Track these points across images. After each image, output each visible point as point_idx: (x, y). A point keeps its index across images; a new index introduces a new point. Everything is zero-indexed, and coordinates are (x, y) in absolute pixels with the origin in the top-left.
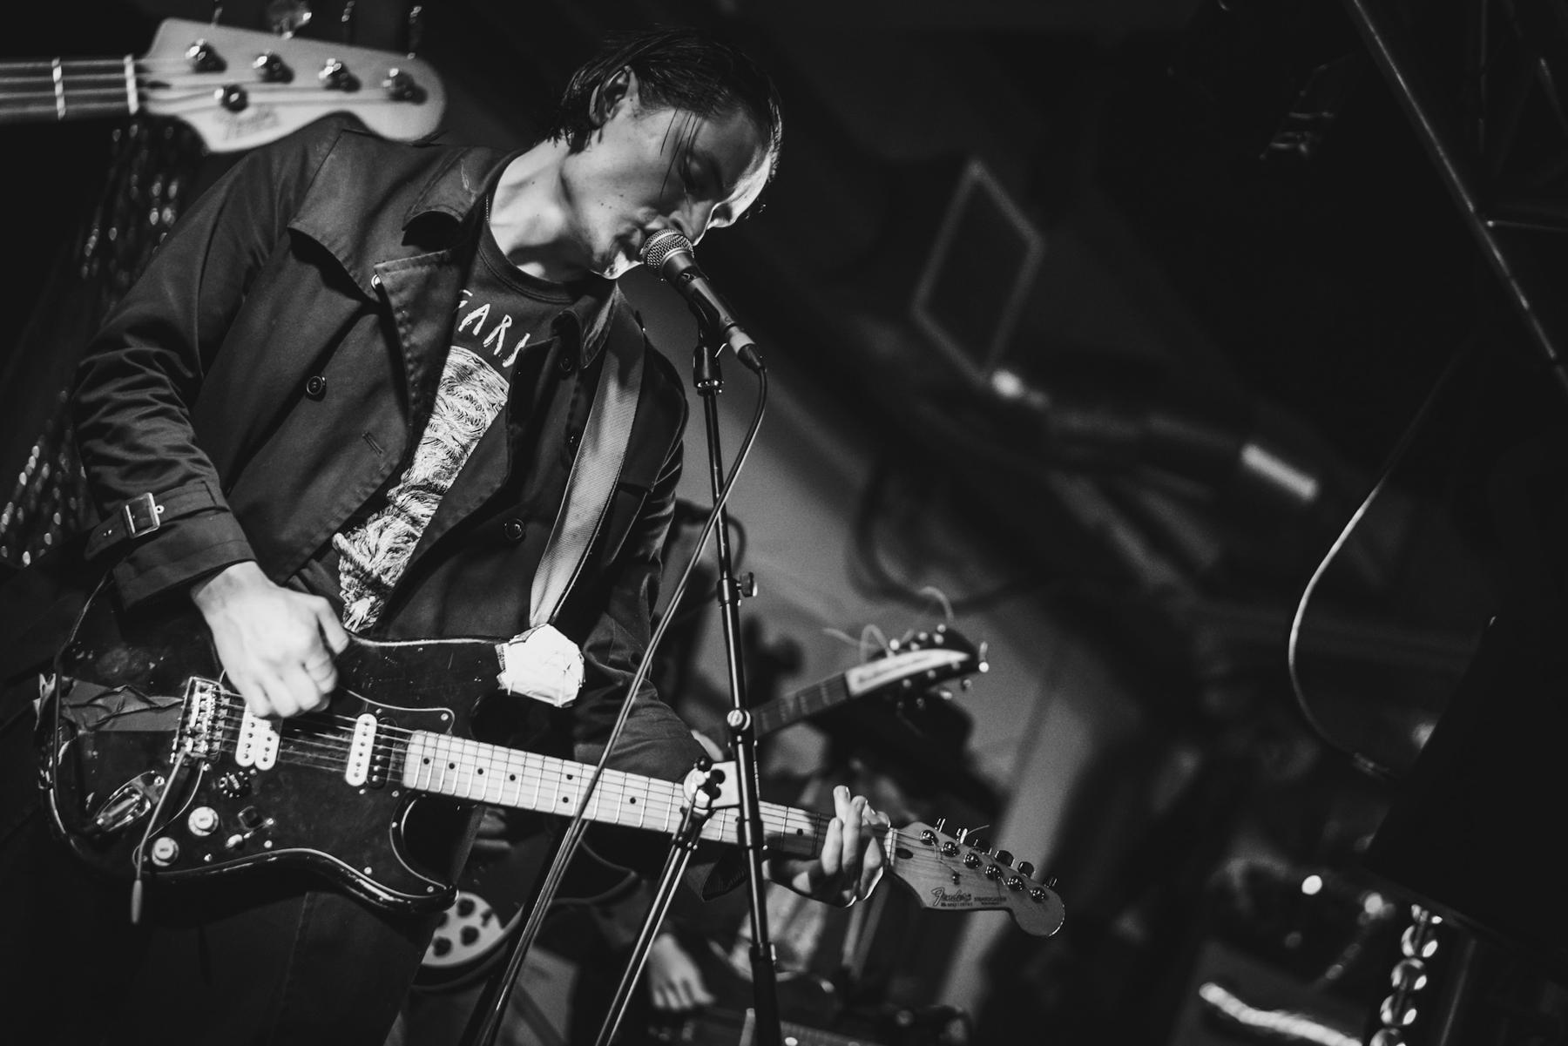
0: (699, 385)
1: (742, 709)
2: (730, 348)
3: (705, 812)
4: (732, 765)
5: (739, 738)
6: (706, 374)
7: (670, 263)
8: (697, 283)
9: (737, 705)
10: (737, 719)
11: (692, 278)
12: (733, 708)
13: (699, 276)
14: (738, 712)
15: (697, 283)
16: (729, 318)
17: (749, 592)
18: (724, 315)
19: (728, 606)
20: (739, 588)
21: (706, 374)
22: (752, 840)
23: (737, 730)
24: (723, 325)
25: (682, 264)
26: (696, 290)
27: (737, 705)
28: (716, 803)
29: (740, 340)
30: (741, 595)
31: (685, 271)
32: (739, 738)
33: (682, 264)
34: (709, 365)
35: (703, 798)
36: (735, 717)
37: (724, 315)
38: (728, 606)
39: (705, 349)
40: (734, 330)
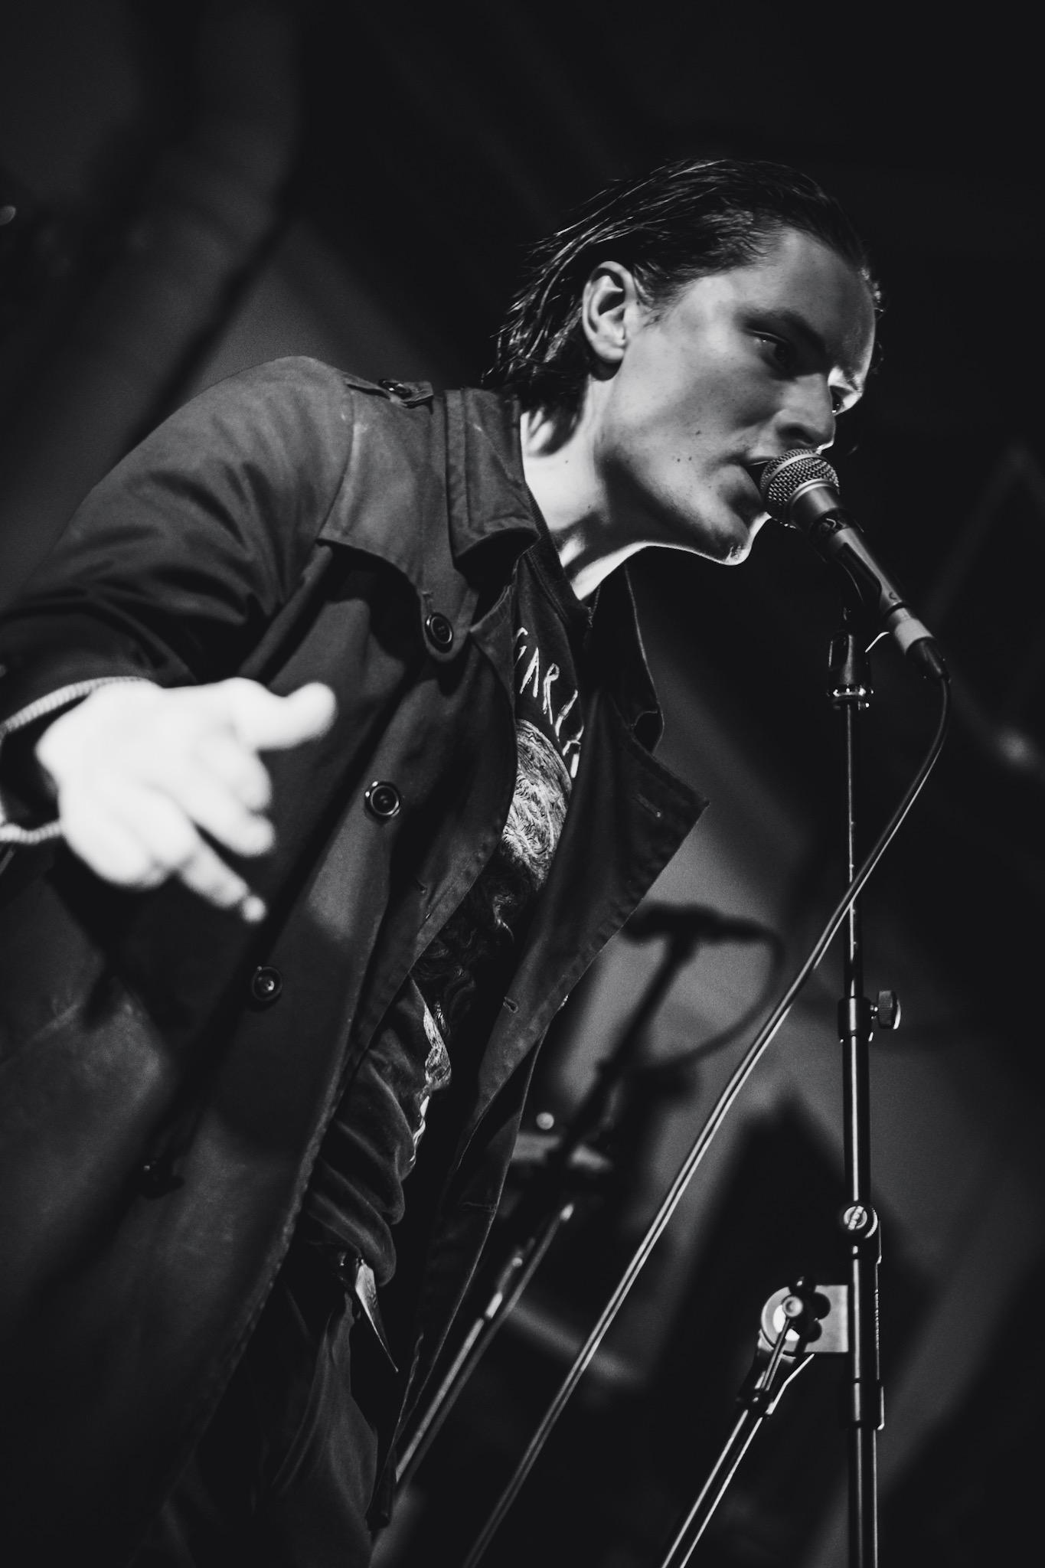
1: (865, 1201)
2: (892, 641)
3: (791, 1359)
5: (855, 1250)
6: (848, 677)
7: (805, 501)
8: (846, 536)
9: (856, 1198)
10: (859, 1221)
11: (839, 528)
13: (851, 525)
14: (860, 1209)
15: (846, 536)
16: (895, 595)
17: (889, 1022)
18: (887, 590)
19: (854, 1039)
20: (874, 1013)
21: (848, 677)
23: (858, 1236)
24: (886, 603)
25: (823, 504)
26: (846, 545)
27: (856, 1198)
29: (910, 630)
31: (830, 514)
32: (855, 1250)
33: (823, 504)
34: (854, 662)
35: (793, 1336)
36: (856, 1216)
37: (887, 590)
38: (854, 1039)
39: (850, 637)
40: (902, 613)
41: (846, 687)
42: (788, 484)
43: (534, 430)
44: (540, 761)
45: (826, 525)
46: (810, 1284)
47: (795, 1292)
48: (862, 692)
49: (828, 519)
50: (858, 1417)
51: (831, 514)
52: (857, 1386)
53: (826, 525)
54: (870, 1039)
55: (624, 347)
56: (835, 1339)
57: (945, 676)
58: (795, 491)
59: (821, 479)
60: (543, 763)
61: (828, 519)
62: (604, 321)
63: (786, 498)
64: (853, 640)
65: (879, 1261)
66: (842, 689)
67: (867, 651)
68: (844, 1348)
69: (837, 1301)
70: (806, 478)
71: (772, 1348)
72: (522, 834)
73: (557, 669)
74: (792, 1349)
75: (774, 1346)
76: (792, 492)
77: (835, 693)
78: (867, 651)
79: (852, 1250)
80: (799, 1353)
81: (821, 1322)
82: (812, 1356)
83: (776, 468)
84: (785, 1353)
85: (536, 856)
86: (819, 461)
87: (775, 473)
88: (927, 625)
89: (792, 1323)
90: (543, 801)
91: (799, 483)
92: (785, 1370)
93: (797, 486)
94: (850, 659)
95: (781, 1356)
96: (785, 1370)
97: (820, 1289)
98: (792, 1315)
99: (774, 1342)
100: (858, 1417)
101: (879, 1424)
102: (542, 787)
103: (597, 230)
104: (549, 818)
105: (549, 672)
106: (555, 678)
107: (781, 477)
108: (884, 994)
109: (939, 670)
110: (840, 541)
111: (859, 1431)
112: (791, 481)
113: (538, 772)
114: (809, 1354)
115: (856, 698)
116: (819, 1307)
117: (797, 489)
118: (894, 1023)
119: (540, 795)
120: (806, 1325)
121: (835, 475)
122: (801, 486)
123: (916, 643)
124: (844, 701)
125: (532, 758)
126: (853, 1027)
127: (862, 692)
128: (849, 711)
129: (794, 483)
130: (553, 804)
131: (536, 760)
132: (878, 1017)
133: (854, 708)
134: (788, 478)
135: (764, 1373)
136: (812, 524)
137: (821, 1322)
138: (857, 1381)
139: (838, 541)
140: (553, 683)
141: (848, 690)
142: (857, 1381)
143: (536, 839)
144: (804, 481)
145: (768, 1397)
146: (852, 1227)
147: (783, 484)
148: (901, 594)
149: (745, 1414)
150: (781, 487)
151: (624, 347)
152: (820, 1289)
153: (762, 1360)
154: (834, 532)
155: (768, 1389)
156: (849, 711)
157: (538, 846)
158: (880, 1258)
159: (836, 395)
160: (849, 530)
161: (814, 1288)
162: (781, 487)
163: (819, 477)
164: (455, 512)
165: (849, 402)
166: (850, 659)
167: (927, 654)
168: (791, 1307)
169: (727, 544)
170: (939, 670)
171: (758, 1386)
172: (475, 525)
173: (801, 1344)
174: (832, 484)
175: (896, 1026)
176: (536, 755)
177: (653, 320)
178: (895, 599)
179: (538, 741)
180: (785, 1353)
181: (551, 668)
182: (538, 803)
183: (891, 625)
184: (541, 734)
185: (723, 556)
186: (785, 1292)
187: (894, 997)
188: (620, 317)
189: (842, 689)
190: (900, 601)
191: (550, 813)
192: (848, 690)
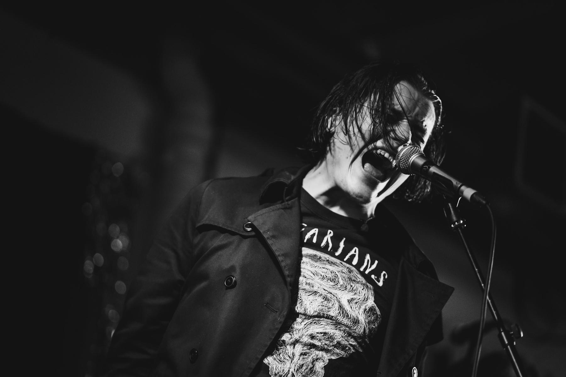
0: (452, 226)
2: (464, 199)
6: (454, 218)
11: (429, 168)
16: (458, 183)
18: (454, 182)
21: (454, 218)
24: (456, 187)
26: (434, 173)
29: (468, 192)
37: (454, 182)
39: (449, 204)
40: (463, 188)
42: (406, 160)
45: (424, 168)
48: (461, 222)
49: (424, 166)
51: (424, 164)
53: (424, 168)
59: (416, 154)
61: (424, 166)
63: (407, 165)
64: (452, 205)
66: (454, 224)
67: (457, 206)
70: (411, 155)
76: (408, 162)
77: (452, 226)
78: (457, 206)
83: (399, 156)
88: (473, 188)
91: (409, 158)
93: (409, 160)
107: (402, 159)
109: (484, 202)
110: (432, 172)
112: (406, 159)
115: (460, 225)
117: (409, 161)
122: (410, 159)
123: (472, 196)
124: (456, 227)
127: (461, 222)
129: (407, 159)
133: (461, 229)
134: (405, 158)
139: (431, 172)
141: (456, 223)
144: (411, 157)
147: (405, 163)
148: (460, 182)
150: (403, 162)
162: (403, 162)
163: (415, 153)
166: (452, 212)
167: (478, 198)
170: (484, 202)
189: (454, 224)
190: (461, 184)
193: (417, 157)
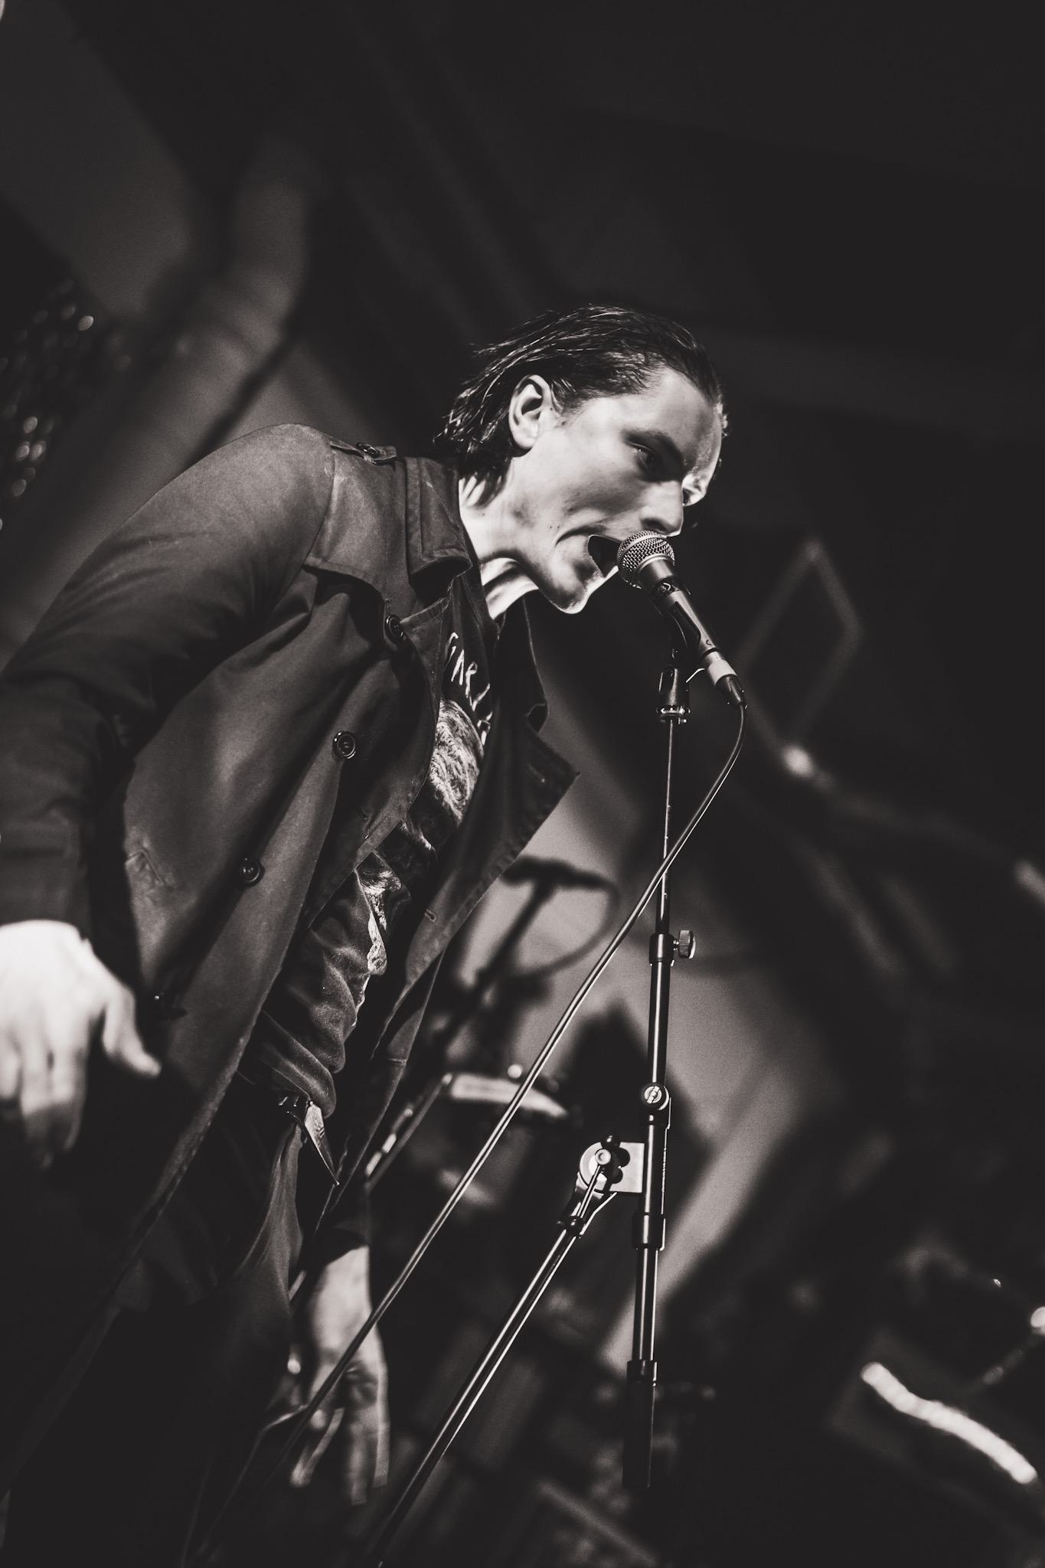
0: (662, 711)
1: (662, 1081)
2: (706, 676)
3: (600, 1196)
4: (641, 1146)
5: (651, 1118)
6: (673, 700)
7: (649, 567)
8: (678, 596)
9: (654, 1080)
10: (655, 1097)
11: (673, 590)
12: (649, 1083)
13: (682, 588)
14: (657, 1088)
15: (678, 596)
16: (710, 642)
18: (705, 637)
19: (660, 964)
20: (676, 946)
21: (673, 700)
22: (649, 1238)
24: (703, 648)
25: (662, 572)
26: (677, 603)
27: (654, 1080)
28: (614, 1188)
29: (720, 668)
30: (676, 955)
31: (667, 580)
32: (651, 1118)
33: (662, 572)
34: (677, 689)
35: (602, 1179)
36: (654, 1094)
37: (705, 637)
38: (660, 964)
39: (676, 670)
40: (715, 656)
41: (670, 707)
43: (469, 490)
44: (462, 733)
46: (617, 1140)
47: (605, 1146)
50: (645, 1241)
52: (646, 1218)
54: (672, 965)
55: (536, 438)
56: (633, 1183)
57: (743, 703)
58: (642, 562)
59: (662, 554)
60: (464, 735)
62: (525, 419)
65: (668, 1128)
66: (668, 708)
68: (639, 1190)
69: (636, 1155)
71: (587, 1187)
72: (449, 785)
73: (476, 666)
74: (601, 1189)
75: (588, 1185)
79: (649, 1118)
80: (606, 1191)
81: (623, 1169)
82: (615, 1193)
84: (596, 1191)
85: (457, 802)
86: (661, 541)
87: (628, 548)
89: (604, 1169)
90: (464, 762)
92: (595, 1203)
94: (674, 686)
95: (593, 1192)
96: (595, 1203)
97: (623, 1145)
98: (602, 1163)
99: (588, 1183)
100: (645, 1241)
101: (661, 1247)
102: (463, 751)
103: (530, 349)
104: (467, 776)
105: (470, 668)
106: (473, 672)
108: (684, 932)
109: (739, 699)
111: (646, 1250)
113: (460, 740)
114: (613, 1193)
115: (677, 715)
116: (623, 1158)
117: (644, 560)
118: (690, 954)
119: (463, 758)
120: (612, 1172)
121: (672, 551)
122: (647, 558)
123: (724, 677)
124: (668, 717)
125: (457, 730)
126: (660, 954)
127: (682, 711)
128: (672, 725)
130: (469, 765)
131: (459, 731)
132: (679, 949)
133: (675, 723)
135: (580, 1204)
136: (653, 586)
137: (623, 1169)
138: (647, 1214)
139: (671, 600)
140: (472, 676)
141: (672, 709)
142: (647, 1214)
143: (458, 789)
145: (581, 1222)
146: (650, 1101)
149: (565, 1232)
151: (536, 438)
152: (623, 1145)
153: (579, 1196)
154: (669, 593)
155: (582, 1217)
156: (672, 725)
157: (459, 795)
158: (669, 1125)
159: (686, 495)
160: (680, 592)
161: (619, 1144)
164: (412, 542)
165: (695, 499)
166: (674, 686)
167: (731, 687)
168: (601, 1157)
169: (569, 598)
170: (739, 699)
171: (574, 1214)
172: (426, 552)
173: (608, 1185)
174: (669, 558)
175: (691, 956)
176: (460, 728)
177: (560, 424)
178: (710, 645)
179: (461, 717)
180: (596, 1191)
181: (472, 665)
182: (461, 763)
183: (707, 664)
184: (463, 712)
185: (566, 607)
186: (598, 1145)
187: (691, 935)
188: (537, 417)
189: (668, 708)
190: (714, 647)
191: (468, 771)
192: (672, 709)
193: (659, 561)
